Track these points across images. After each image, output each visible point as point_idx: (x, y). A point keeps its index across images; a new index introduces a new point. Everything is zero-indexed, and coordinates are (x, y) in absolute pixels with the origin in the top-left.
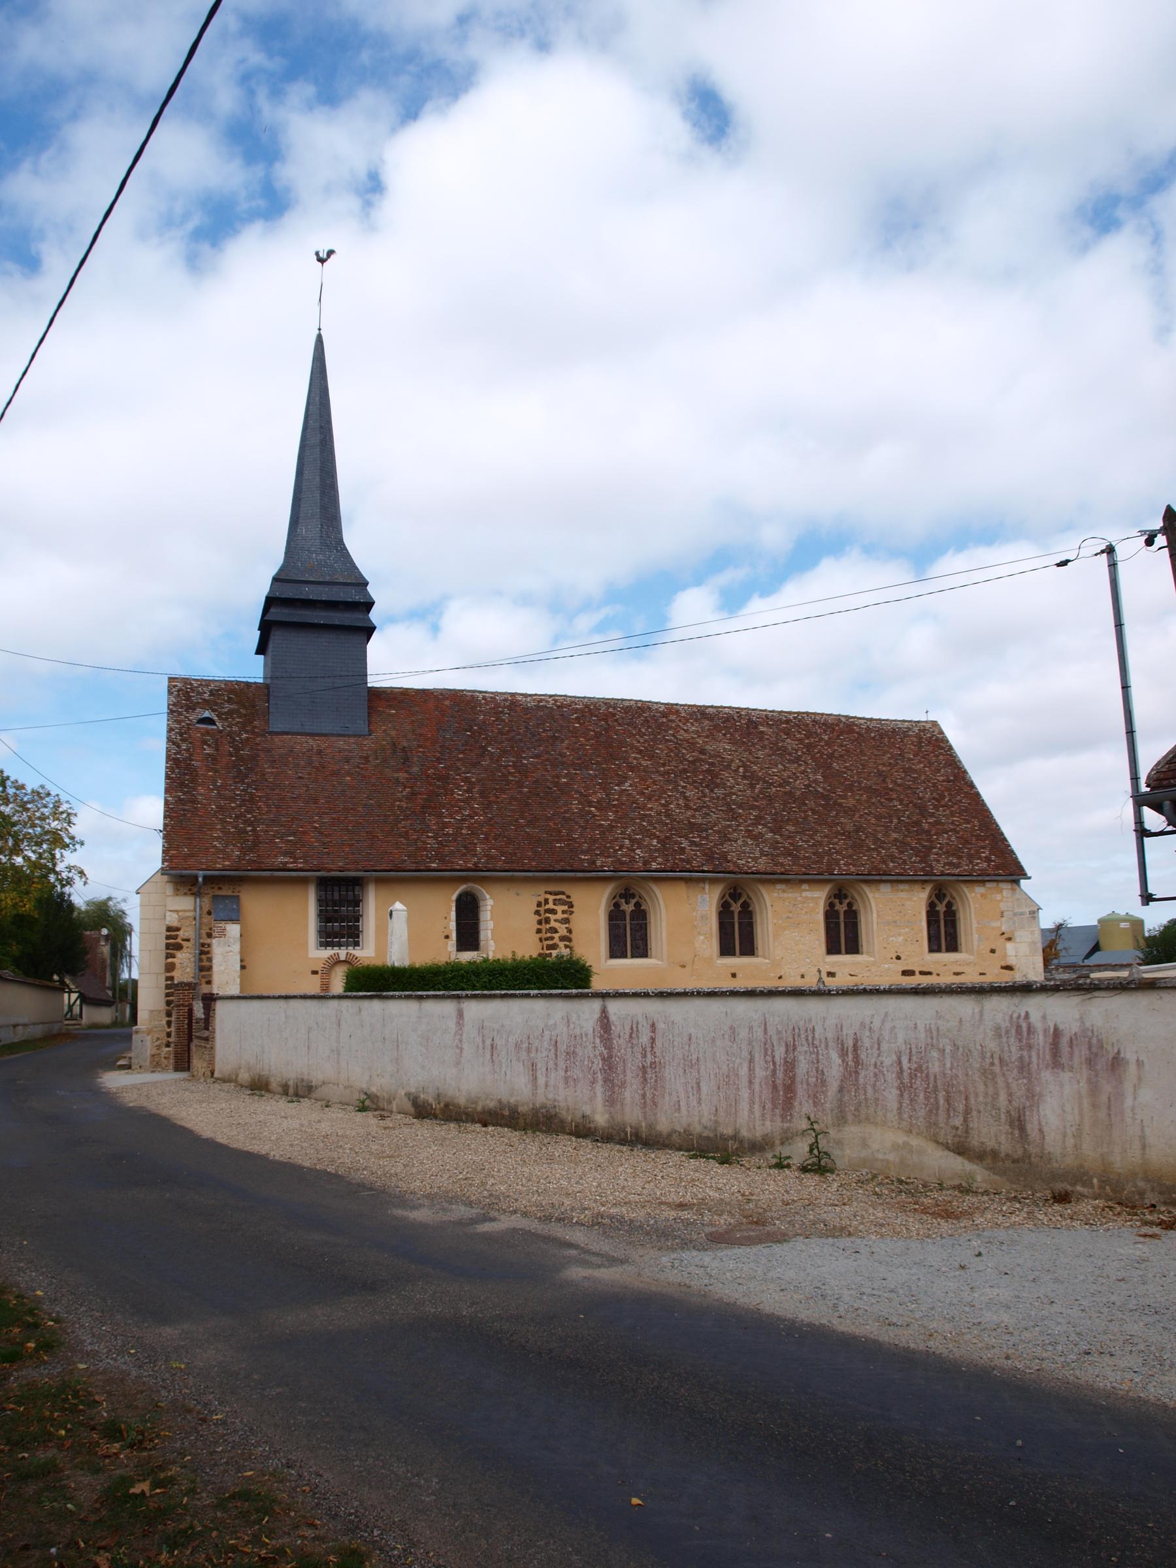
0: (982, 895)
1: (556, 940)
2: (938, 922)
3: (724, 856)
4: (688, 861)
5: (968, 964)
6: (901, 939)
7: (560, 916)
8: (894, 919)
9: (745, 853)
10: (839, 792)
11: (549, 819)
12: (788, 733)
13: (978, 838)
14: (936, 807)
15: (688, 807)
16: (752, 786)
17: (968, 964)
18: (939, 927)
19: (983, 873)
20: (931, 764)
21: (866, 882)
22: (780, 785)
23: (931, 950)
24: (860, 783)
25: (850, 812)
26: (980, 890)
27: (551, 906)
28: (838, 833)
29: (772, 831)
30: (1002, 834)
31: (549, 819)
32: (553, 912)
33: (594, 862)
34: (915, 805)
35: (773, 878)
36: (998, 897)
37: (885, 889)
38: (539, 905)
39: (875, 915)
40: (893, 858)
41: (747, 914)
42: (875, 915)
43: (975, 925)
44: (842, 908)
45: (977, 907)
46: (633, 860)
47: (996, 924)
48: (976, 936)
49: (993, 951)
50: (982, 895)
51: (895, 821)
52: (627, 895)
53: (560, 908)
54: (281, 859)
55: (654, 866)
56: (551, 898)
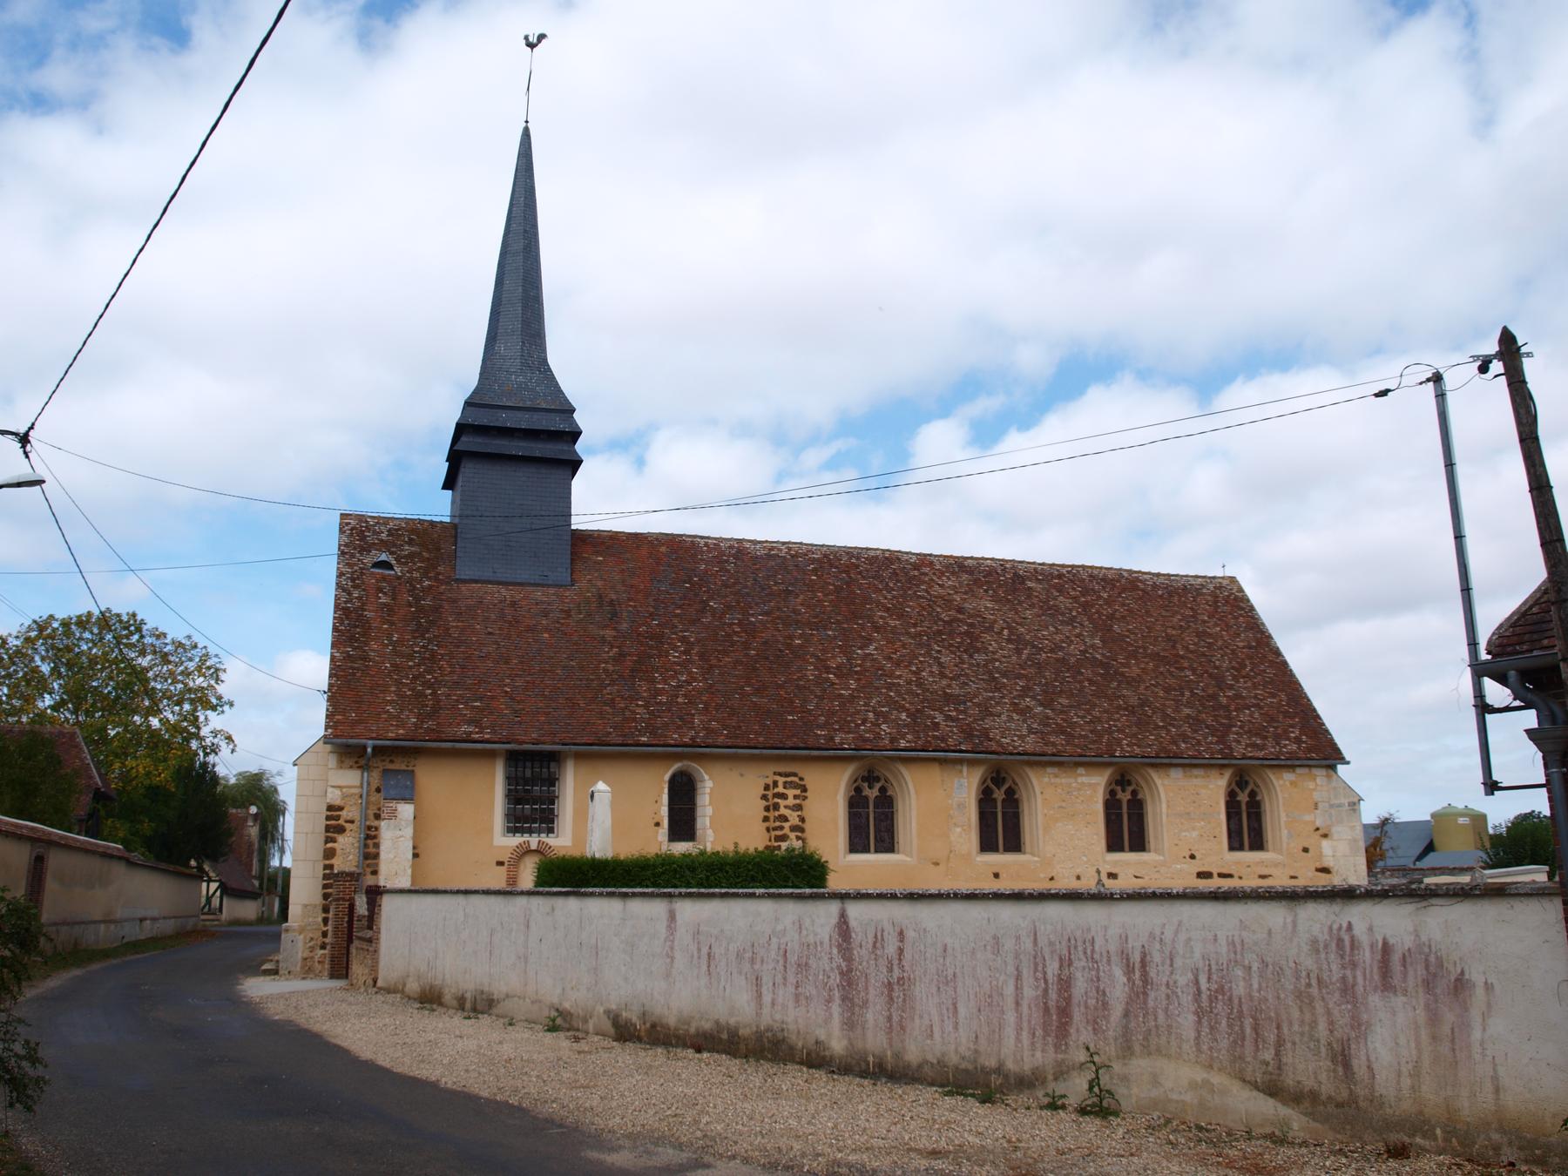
1: (786, 831)
2: (1239, 814)
4: (943, 739)
5: (1276, 865)
6: (1195, 834)
7: (791, 801)
12: (1060, 590)
14: (1235, 678)
15: (943, 675)
17: (1276, 865)
18: (1240, 820)
19: (1292, 756)
21: (1153, 765)
22: (1052, 651)
23: (1231, 848)
25: (1132, 682)
26: (1288, 776)
27: (780, 789)
28: (1119, 707)
31: (781, 687)
33: (832, 739)
34: (1211, 675)
36: (1311, 785)
37: (1176, 774)
38: (767, 788)
39: (1164, 806)
40: (1185, 738)
42: (1164, 806)
43: (1283, 818)
45: (1286, 796)
46: (878, 736)
47: (1308, 818)
48: (1285, 832)
49: (1306, 850)
53: (791, 793)
55: (903, 744)
56: (781, 780)
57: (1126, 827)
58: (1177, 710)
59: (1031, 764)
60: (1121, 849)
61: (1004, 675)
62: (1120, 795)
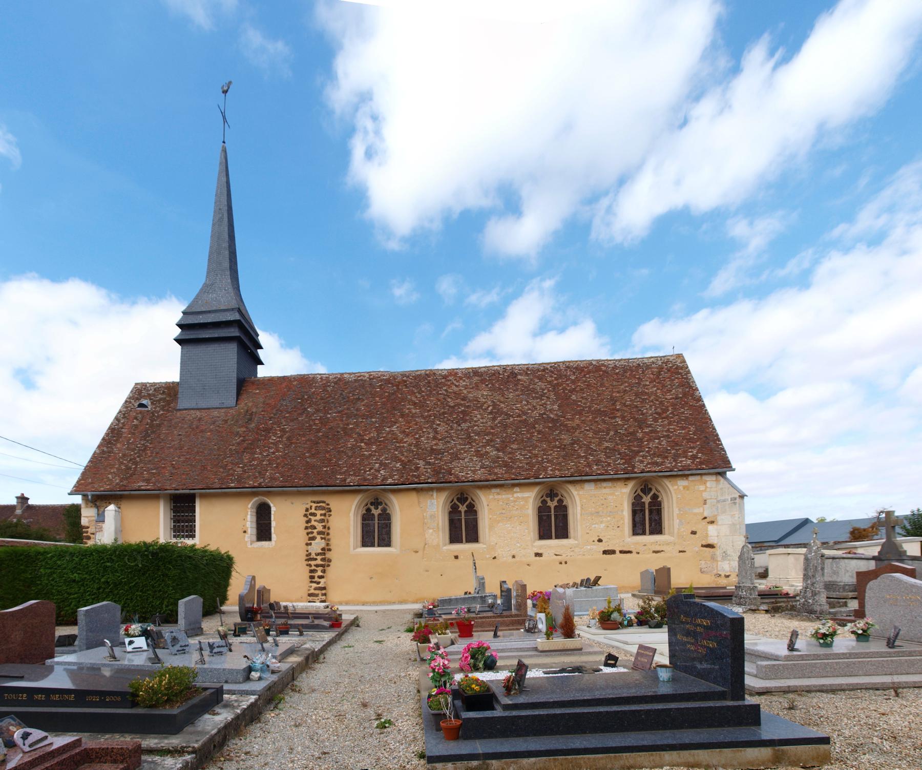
0: (684, 487)
1: (315, 534)
2: (643, 511)
3: (456, 471)
4: (418, 477)
5: (668, 544)
6: (602, 526)
7: (318, 517)
8: (601, 510)
9: (468, 467)
10: (569, 416)
11: (328, 452)
12: (541, 378)
13: (690, 440)
14: (656, 420)
15: (435, 438)
16: (494, 419)
17: (668, 544)
22: (519, 416)
25: (568, 430)
26: (682, 483)
27: (313, 511)
28: (556, 446)
29: (498, 450)
31: (328, 452)
32: (314, 515)
33: (345, 480)
34: (636, 420)
35: (488, 485)
36: (702, 488)
37: (589, 488)
38: (307, 510)
39: (579, 508)
40: (598, 462)
41: (472, 510)
42: (579, 508)
43: (676, 511)
44: (552, 504)
46: (376, 477)
47: (696, 511)
48: (676, 522)
49: (694, 533)
50: (684, 487)
51: (612, 433)
52: (376, 503)
53: (319, 512)
55: (390, 481)
56: (314, 505)
57: (553, 523)
58: (600, 444)
59: (480, 488)
60: (550, 538)
61: (478, 434)
62: (550, 503)
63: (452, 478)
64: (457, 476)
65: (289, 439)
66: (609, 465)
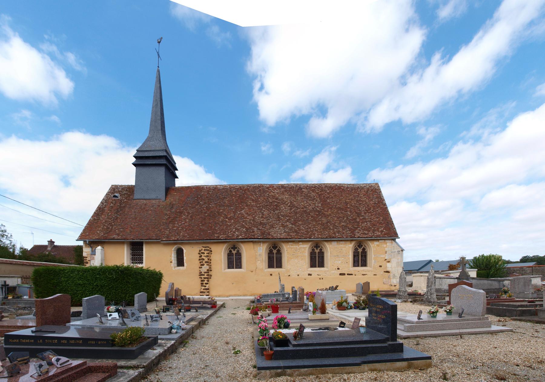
0: (377, 245)
1: (204, 263)
2: (358, 255)
3: (272, 233)
4: (254, 236)
5: (369, 271)
6: (340, 262)
7: (206, 255)
8: (339, 254)
9: (278, 232)
10: (326, 210)
11: (210, 223)
12: (313, 191)
13: (381, 223)
14: (365, 213)
15: (262, 217)
16: (291, 209)
17: (369, 271)
18: (359, 257)
19: (378, 236)
20: (369, 198)
21: (326, 241)
22: (303, 208)
23: (354, 265)
24: (336, 206)
25: (326, 216)
26: (376, 243)
27: (203, 251)
28: (319, 224)
29: (292, 224)
30: (392, 222)
31: (210, 223)
32: (203, 253)
33: (219, 237)
34: (356, 213)
35: (288, 240)
36: (385, 246)
37: (334, 244)
38: (200, 251)
39: (329, 253)
40: (339, 232)
41: (279, 252)
42: (329, 253)
43: (373, 256)
44: (317, 251)
45: (375, 250)
46: (233, 235)
47: (382, 256)
48: (373, 261)
49: (381, 266)
50: (377, 245)
51: (345, 218)
52: (234, 248)
53: (206, 252)
54: (115, 236)
55: (240, 237)
56: (203, 249)
57: (317, 260)
58: (340, 223)
59: (284, 242)
60: (315, 267)
61: (283, 216)
62: (316, 251)
63: (270, 237)
64: (272, 236)
65: (191, 217)
66: (344, 233)
